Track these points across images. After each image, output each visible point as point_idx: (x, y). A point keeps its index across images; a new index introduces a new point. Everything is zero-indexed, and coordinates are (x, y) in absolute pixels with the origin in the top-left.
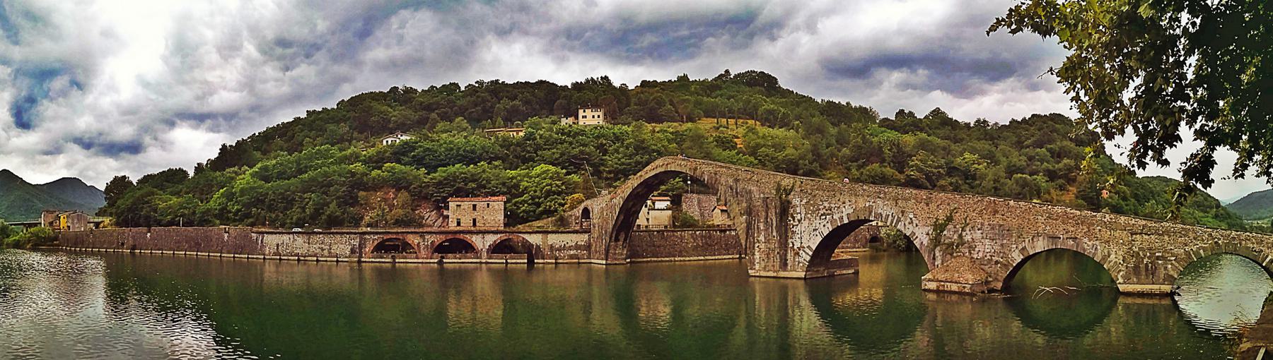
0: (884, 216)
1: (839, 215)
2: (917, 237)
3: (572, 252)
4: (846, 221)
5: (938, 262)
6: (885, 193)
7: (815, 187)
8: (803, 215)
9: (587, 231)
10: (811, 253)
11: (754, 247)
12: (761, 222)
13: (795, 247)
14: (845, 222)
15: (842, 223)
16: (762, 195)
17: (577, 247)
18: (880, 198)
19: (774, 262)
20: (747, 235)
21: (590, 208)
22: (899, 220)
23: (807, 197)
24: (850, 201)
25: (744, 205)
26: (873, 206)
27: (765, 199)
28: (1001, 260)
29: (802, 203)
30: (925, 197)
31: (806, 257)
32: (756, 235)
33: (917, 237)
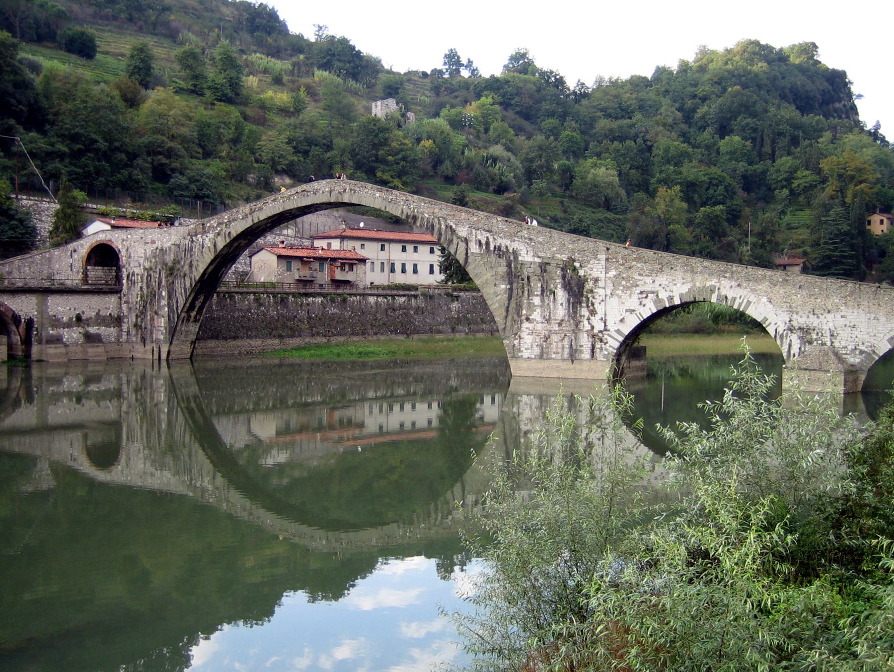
0: (729, 298)
1: (669, 294)
2: (770, 324)
3: (93, 330)
4: (677, 302)
5: (795, 350)
6: (732, 273)
7: (631, 257)
8: (609, 292)
9: (114, 288)
10: (621, 339)
11: (519, 329)
12: (534, 295)
13: (596, 331)
14: (676, 303)
15: (671, 305)
16: (537, 260)
17: (101, 320)
18: (726, 277)
19: (557, 347)
20: (507, 311)
21: (118, 245)
22: (749, 303)
23: (616, 269)
24: (683, 279)
25: (503, 269)
26: (715, 287)
27: (544, 267)
28: (866, 350)
29: (607, 275)
30: (781, 280)
31: (613, 343)
32: (524, 312)
33: (770, 324)
